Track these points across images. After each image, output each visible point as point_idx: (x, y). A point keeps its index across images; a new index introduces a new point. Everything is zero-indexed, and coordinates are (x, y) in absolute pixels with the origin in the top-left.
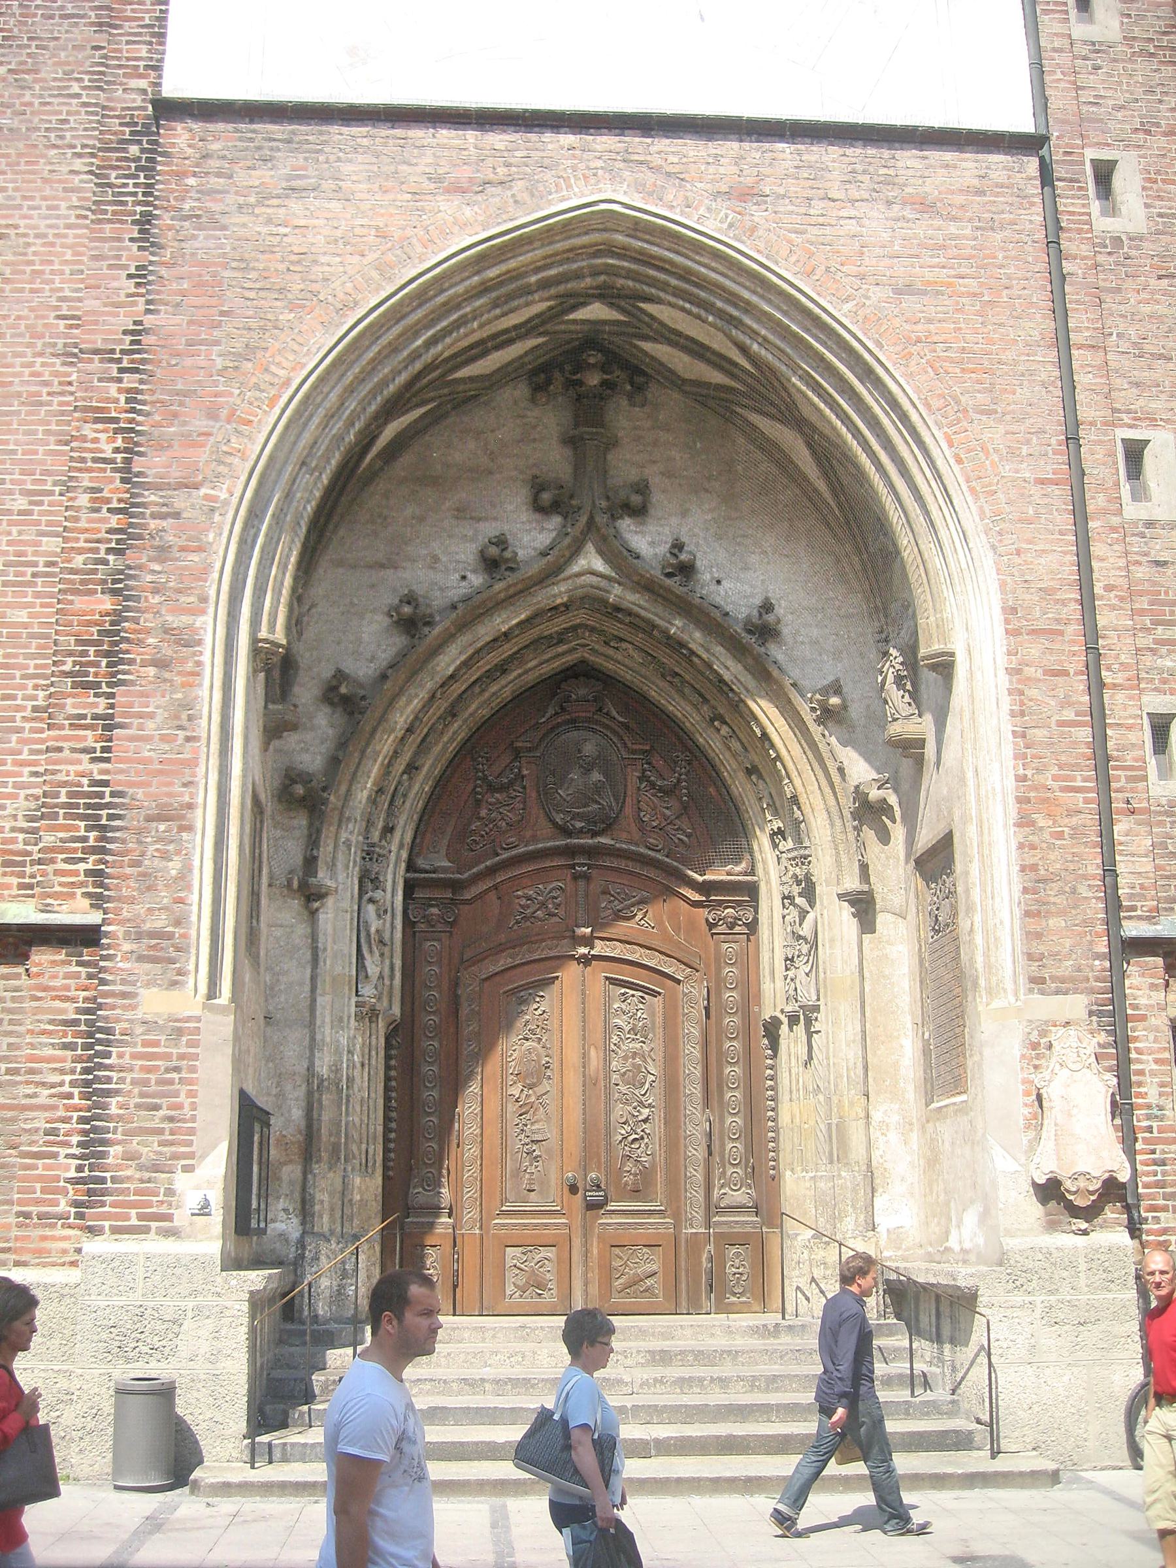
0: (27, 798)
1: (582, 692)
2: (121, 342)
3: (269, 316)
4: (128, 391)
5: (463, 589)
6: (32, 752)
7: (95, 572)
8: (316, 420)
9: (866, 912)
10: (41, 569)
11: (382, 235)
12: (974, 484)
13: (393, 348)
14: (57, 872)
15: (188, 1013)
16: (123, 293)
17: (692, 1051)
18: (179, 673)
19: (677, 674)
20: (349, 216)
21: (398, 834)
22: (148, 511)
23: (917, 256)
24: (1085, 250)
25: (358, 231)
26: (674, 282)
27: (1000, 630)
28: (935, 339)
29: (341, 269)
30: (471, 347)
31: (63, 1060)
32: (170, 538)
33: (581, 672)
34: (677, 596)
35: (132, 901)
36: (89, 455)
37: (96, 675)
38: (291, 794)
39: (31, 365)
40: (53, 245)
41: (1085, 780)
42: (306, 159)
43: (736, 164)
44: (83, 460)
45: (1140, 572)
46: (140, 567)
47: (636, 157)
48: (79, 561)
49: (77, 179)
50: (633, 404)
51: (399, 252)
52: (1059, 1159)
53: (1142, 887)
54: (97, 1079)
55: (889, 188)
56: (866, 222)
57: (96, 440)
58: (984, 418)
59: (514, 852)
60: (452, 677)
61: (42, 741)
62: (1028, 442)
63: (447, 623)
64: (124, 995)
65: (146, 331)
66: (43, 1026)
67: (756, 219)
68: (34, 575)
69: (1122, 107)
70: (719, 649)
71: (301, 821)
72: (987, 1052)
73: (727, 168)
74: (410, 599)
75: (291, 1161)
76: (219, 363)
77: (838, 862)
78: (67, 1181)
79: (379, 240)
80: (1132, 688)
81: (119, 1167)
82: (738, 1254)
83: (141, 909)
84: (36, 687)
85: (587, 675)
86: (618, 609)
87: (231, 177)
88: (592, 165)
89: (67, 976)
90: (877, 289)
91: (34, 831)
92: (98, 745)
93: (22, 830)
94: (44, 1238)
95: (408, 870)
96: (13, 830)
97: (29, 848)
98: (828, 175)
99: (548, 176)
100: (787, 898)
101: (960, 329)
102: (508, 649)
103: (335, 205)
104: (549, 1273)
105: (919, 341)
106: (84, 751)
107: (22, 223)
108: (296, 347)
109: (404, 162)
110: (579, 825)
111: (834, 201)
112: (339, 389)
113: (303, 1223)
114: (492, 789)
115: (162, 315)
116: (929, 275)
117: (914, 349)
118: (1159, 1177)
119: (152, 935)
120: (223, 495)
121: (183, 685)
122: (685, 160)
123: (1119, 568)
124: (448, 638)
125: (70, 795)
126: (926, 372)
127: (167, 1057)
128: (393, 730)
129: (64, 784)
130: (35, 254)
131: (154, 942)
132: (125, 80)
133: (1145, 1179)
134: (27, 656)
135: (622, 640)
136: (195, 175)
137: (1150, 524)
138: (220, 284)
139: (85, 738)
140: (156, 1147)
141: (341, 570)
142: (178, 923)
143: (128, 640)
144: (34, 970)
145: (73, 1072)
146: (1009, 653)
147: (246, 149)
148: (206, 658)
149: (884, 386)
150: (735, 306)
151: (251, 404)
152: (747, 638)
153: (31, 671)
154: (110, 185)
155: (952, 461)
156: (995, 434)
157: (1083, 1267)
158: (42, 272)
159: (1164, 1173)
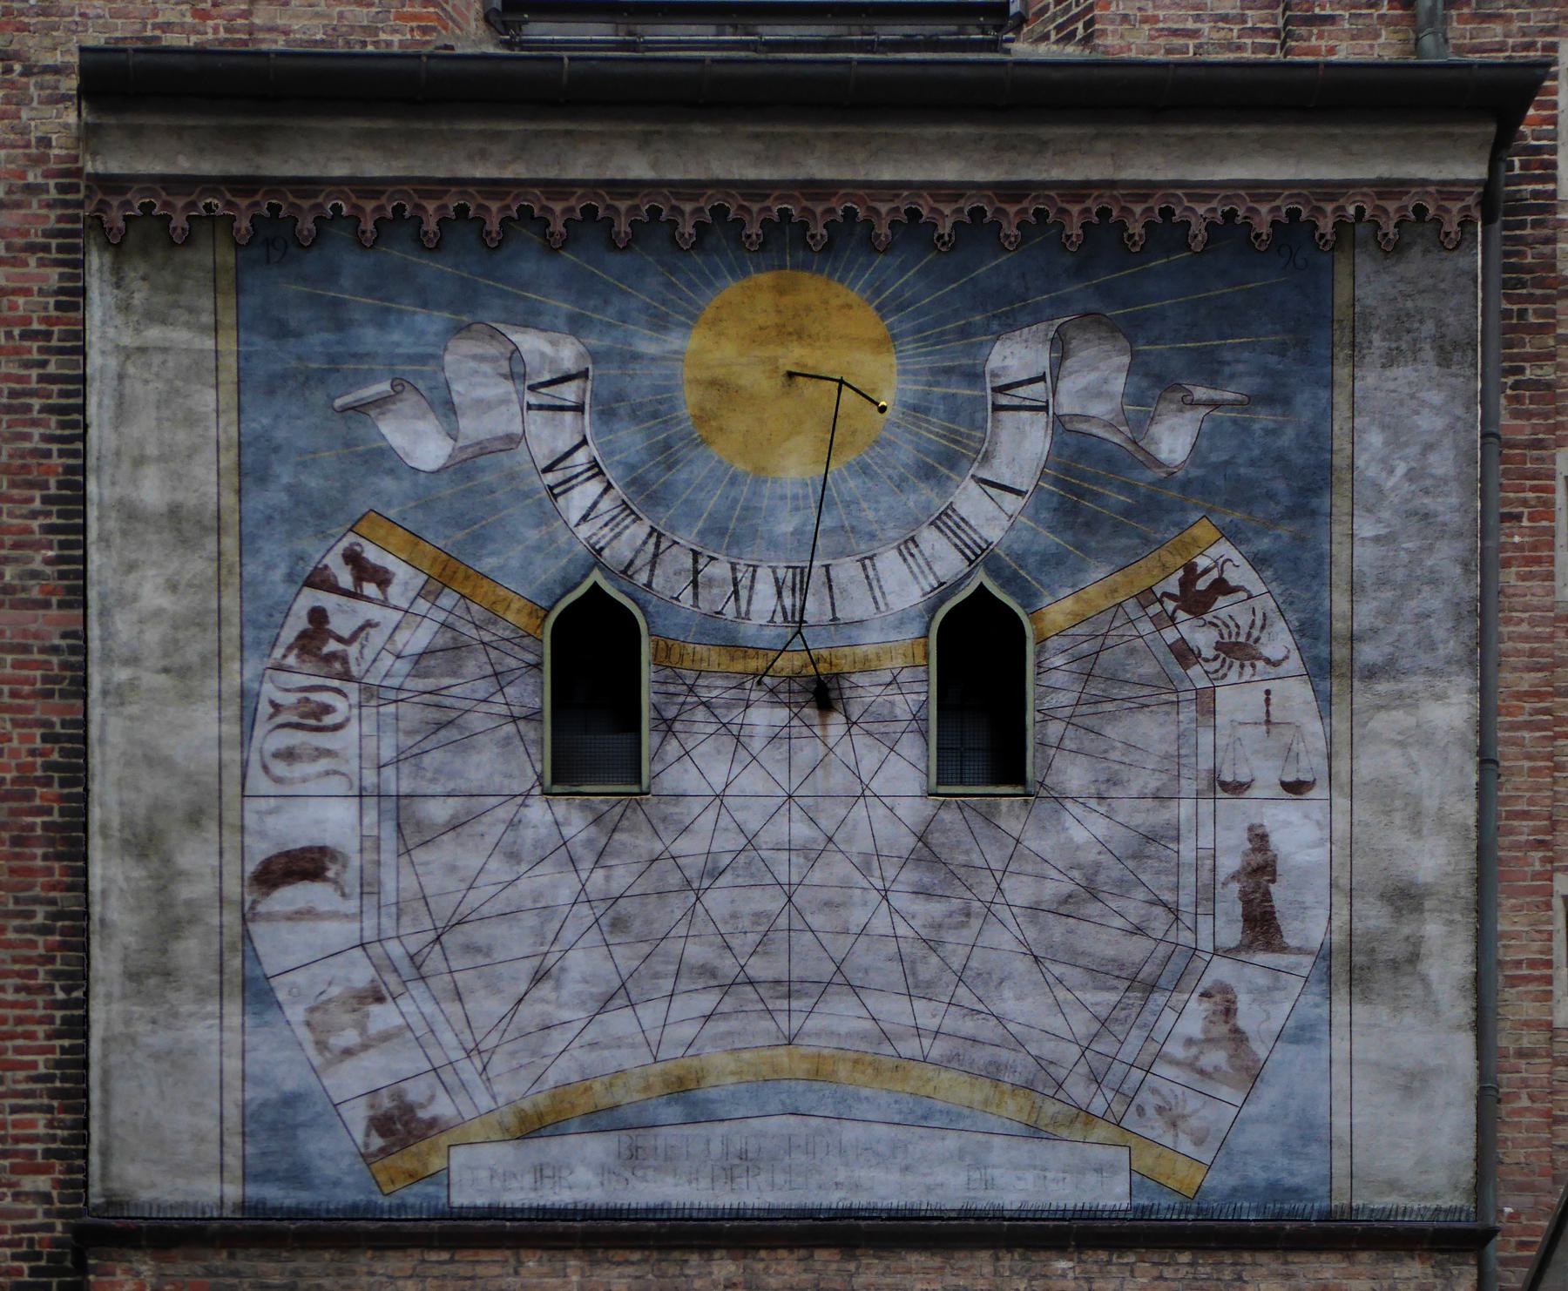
132: (14, 1178)
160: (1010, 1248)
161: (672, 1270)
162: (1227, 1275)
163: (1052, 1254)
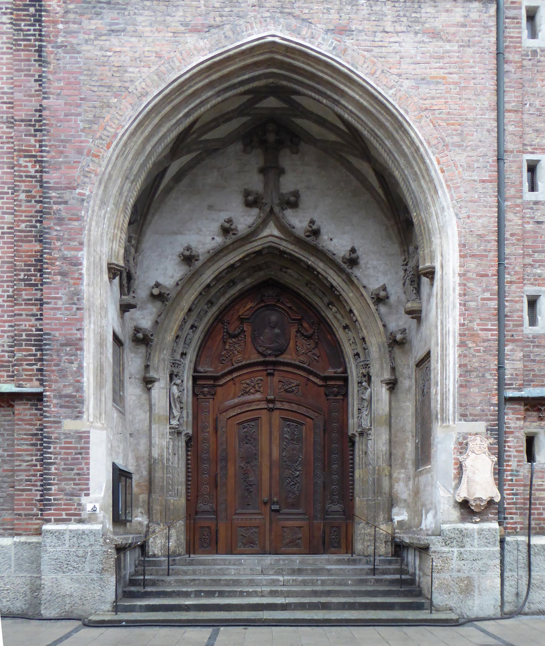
0: (8, 337)
3: (105, 101)
6: (8, 316)
7: (31, 231)
8: (130, 156)
10: (6, 230)
11: (159, 56)
12: (449, 183)
13: (167, 117)
14: (24, 370)
20: (141, 46)
23: (428, 63)
25: (146, 54)
27: (457, 255)
28: (435, 107)
29: (139, 75)
31: (32, 450)
35: (56, 381)
37: (35, 280)
42: (118, 13)
43: (338, 13)
45: (528, 227)
47: (286, 10)
48: (23, 226)
51: (167, 65)
55: (417, 24)
56: (403, 44)
58: (457, 149)
61: (13, 311)
65: (45, 109)
66: (22, 436)
67: (347, 44)
72: (439, 446)
76: (82, 125)
78: (36, 500)
79: (157, 59)
80: (519, 283)
83: (61, 385)
84: (8, 286)
87: (80, 24)
88: (264, 15)
89: (31, 415)
90: (407, 81)
91: (12, 352)
92: (39, 313)
93: (7, 351)
94: (28, 524)
97: (10, 359)
98: (385, 18)
99: (242, 22)
101: (448, 102)
103: (133, 39)
105: (426, 109)
106: (33, 315)
108: (119, 117)
109: (168, 15)
111: (387, 32)
112: (141, 139)
115: (51, 100)
116: (434, 73)
117: (423, 114)
118: (514, 500)
122: (311, 11)
123: (519, 225)
126: (429, 125)
129: (24, 330)
133: (508, 501)
136: (62, 22)
137: (536, 203)
138: (79, 84)
139: (32, 310)
144: (16, 412)
145: (36, 455)
146: (460, 266)
147: (87, 8)
149: (408, 134)
151: (98, 147)
153: (5, 279)
155: (439, 172)
156: (461, 158)
159: (517, 499)
162: (416, 6)
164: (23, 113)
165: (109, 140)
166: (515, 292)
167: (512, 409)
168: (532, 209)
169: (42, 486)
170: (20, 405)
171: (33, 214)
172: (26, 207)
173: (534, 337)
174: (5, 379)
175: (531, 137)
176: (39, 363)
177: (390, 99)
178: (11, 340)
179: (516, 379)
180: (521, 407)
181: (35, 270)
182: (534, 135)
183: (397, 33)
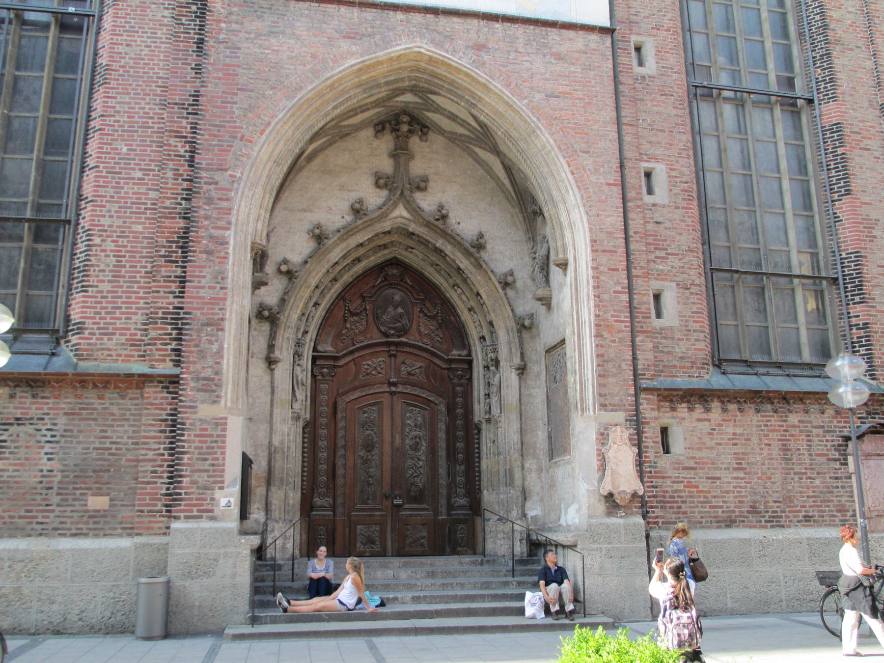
1: (395, 271)
2: (188, 100)
4: (191, 123)
5: (342, 223)
7: (175, 208)
9: (522, 374)
11: (314, 56)
14: (157, 350)
15: (221, 415)
16: (189, 77)
17: (442, 435)
18: (218, 257)
19: (437, 265)
21: (309, 335)
22: (202, 181)
24: (630, 81)
26: (446, 86)
30: (349, 111)
31: (160, 438)
32: (213, 194)
33: (394, 262)
34: (441, 230)
36: (172, 153)
37: (176, 257)
38: (262, 316)
39: (144, 108)
40: (154, 51)
41: (625, 317)
44: (170, 155)
45: (650, 227)
46: (199, 207)
48: (168, 203)
49: (166, 20)
50: (421, 140)
52: (613, 484)
53: (648, 365)
54: (178, 447)
57: (176, 146)
59: (362, 344)
60: (336, 263)
61: (150, 288)
62: (603, 166)
63: (336, 238)
64: (190, 407)
68: (146, 209)
69: (648, 17)
70: (459, 254)
71: (266, 327)
73: (473, 35)
74: (318, 226)
75: (260, 486)
77: (511, 353)
78: (162, 495)
81: (188, 488)
82: (462, 528)
84: (146, 262)
85: (398, 265)
86: (413, 234)
87: (242, 24)
89: (162, 398)
91: (146, 330)
92: (177, 290)
94: (150, 522)
95: (313, 351)
96: (136, 329)
99: (391, 34)
100: (487, 368)
102: (362, 251)
103: (292, 41)
104: (376, 536)
106: (171, 292)
107: (139, 39)
110: (392, 332)
113: (267, 514)
114: (353, 314)
116: (561, 89)
117: (554, 122)
119: (205, 379)
120: (238, 175)
121: (220, 263)
124: (336, 244)
125: (164, 313)
127: (211, 436)
128: (309, 287)
129: (161, 308)
130: (145, 55)
131: (205, 382)
134: (142, 247)
135: (413, 248)
136: (225, 22)
137: (654, 205)
139: (170, 287)
140: (206, 478)
141: (286, 212)
142: (217, 374)
143: (193, 241)
144: (146, 395)
145: (165, 443)
146: (593, 260)
148: (231, 251)
150: (474, 98)
152: (472, 250)
153: (144, 254)
154: (182, 24)
156: (588, 162)
157: (623, 532)
158: (148, 64)
159: (657, 492)
160: (483, 19)
161: (385, 15)
163: (495, 23)
164: (177, 97)
165: (262, 128)
166: (642, 286)
167: (646, 399)
168: (651, 210)
169: (169, 478)
170: (150, 387)
171: (180, 191)
172: (173, 184)
173: (661, 329)
174: (136, 358)
175: (645, 147)
176: (174, 343)
177: (524, 109)
178: (145, 317)
179: (648, 370)
180: (653, 398)
181: (177, 247)
182: (648, 146)
183: (528, 54)
